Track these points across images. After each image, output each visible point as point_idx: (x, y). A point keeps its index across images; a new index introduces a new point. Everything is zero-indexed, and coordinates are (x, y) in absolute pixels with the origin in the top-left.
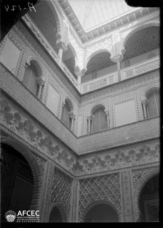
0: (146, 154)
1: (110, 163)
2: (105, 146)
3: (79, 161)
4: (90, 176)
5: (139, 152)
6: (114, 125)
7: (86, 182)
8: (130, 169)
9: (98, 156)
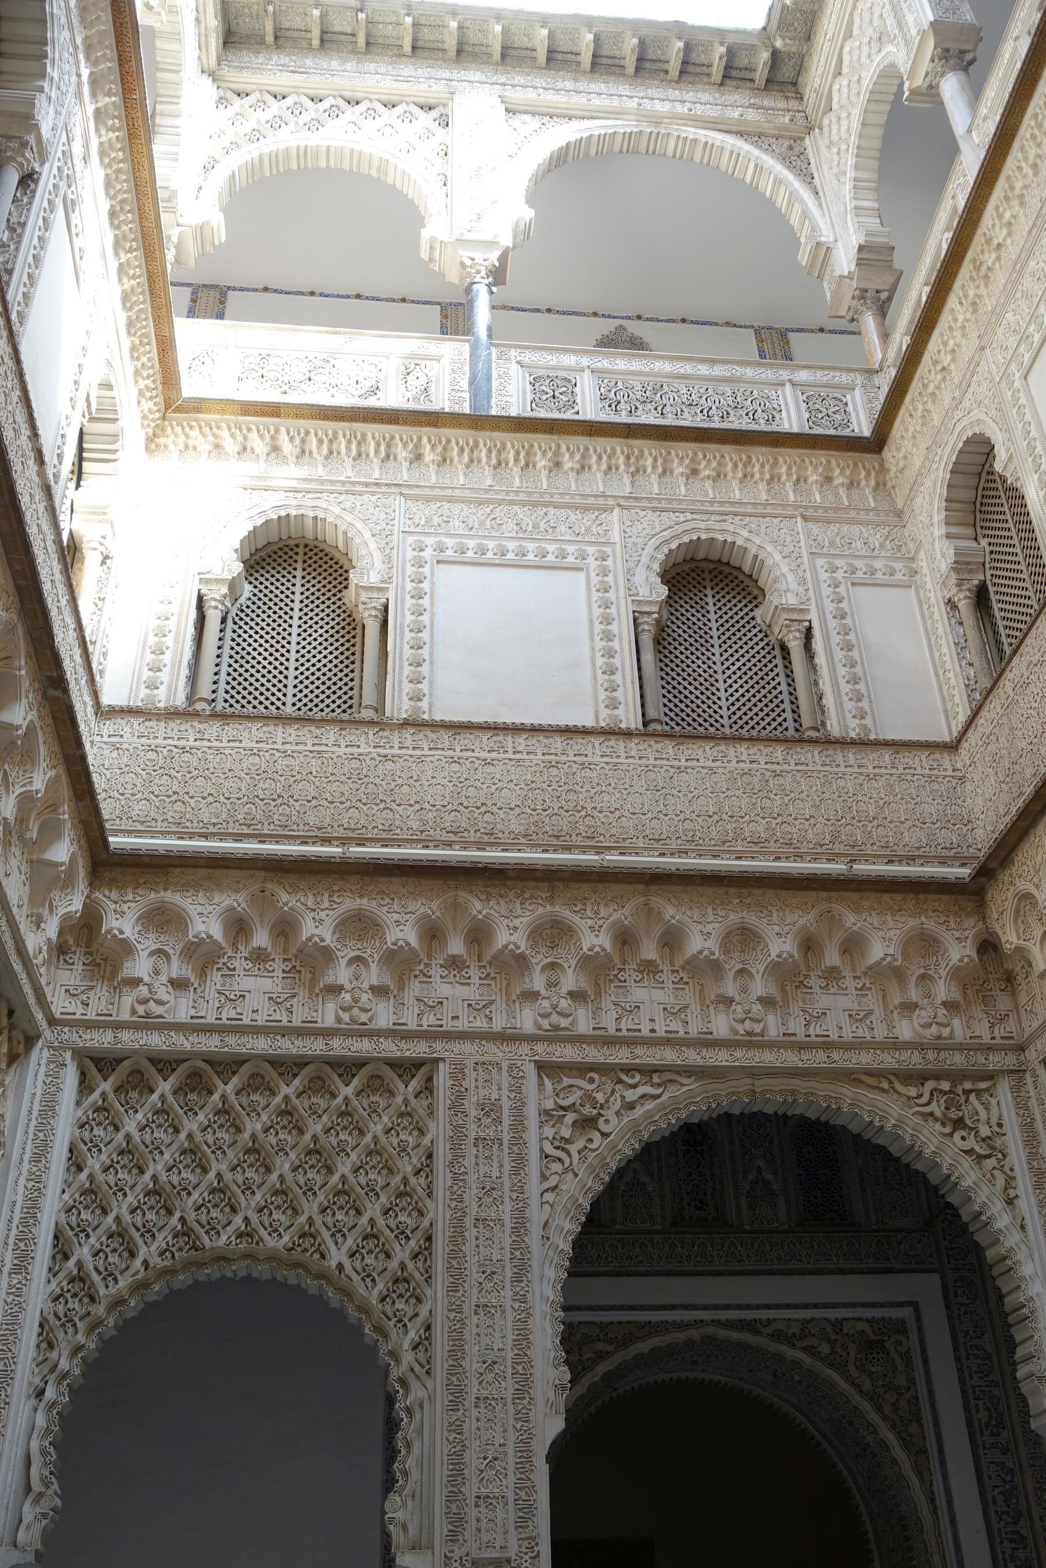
0: (649, 968)
1: (374, 975)
2: (340, 833)
3: (107, 899)
4: (185, 1043)
5: (608, 946)
6: (424, 704)
7: (137, 1083)
8: (525, 1048)
9: (284, 897)
